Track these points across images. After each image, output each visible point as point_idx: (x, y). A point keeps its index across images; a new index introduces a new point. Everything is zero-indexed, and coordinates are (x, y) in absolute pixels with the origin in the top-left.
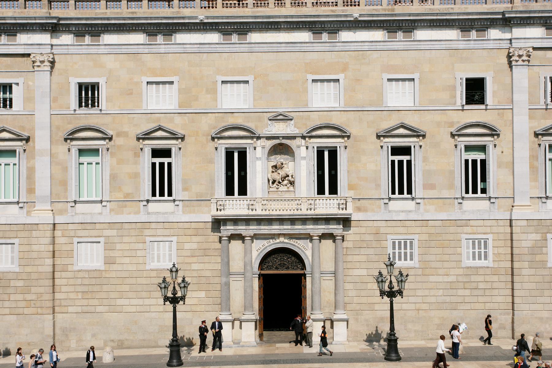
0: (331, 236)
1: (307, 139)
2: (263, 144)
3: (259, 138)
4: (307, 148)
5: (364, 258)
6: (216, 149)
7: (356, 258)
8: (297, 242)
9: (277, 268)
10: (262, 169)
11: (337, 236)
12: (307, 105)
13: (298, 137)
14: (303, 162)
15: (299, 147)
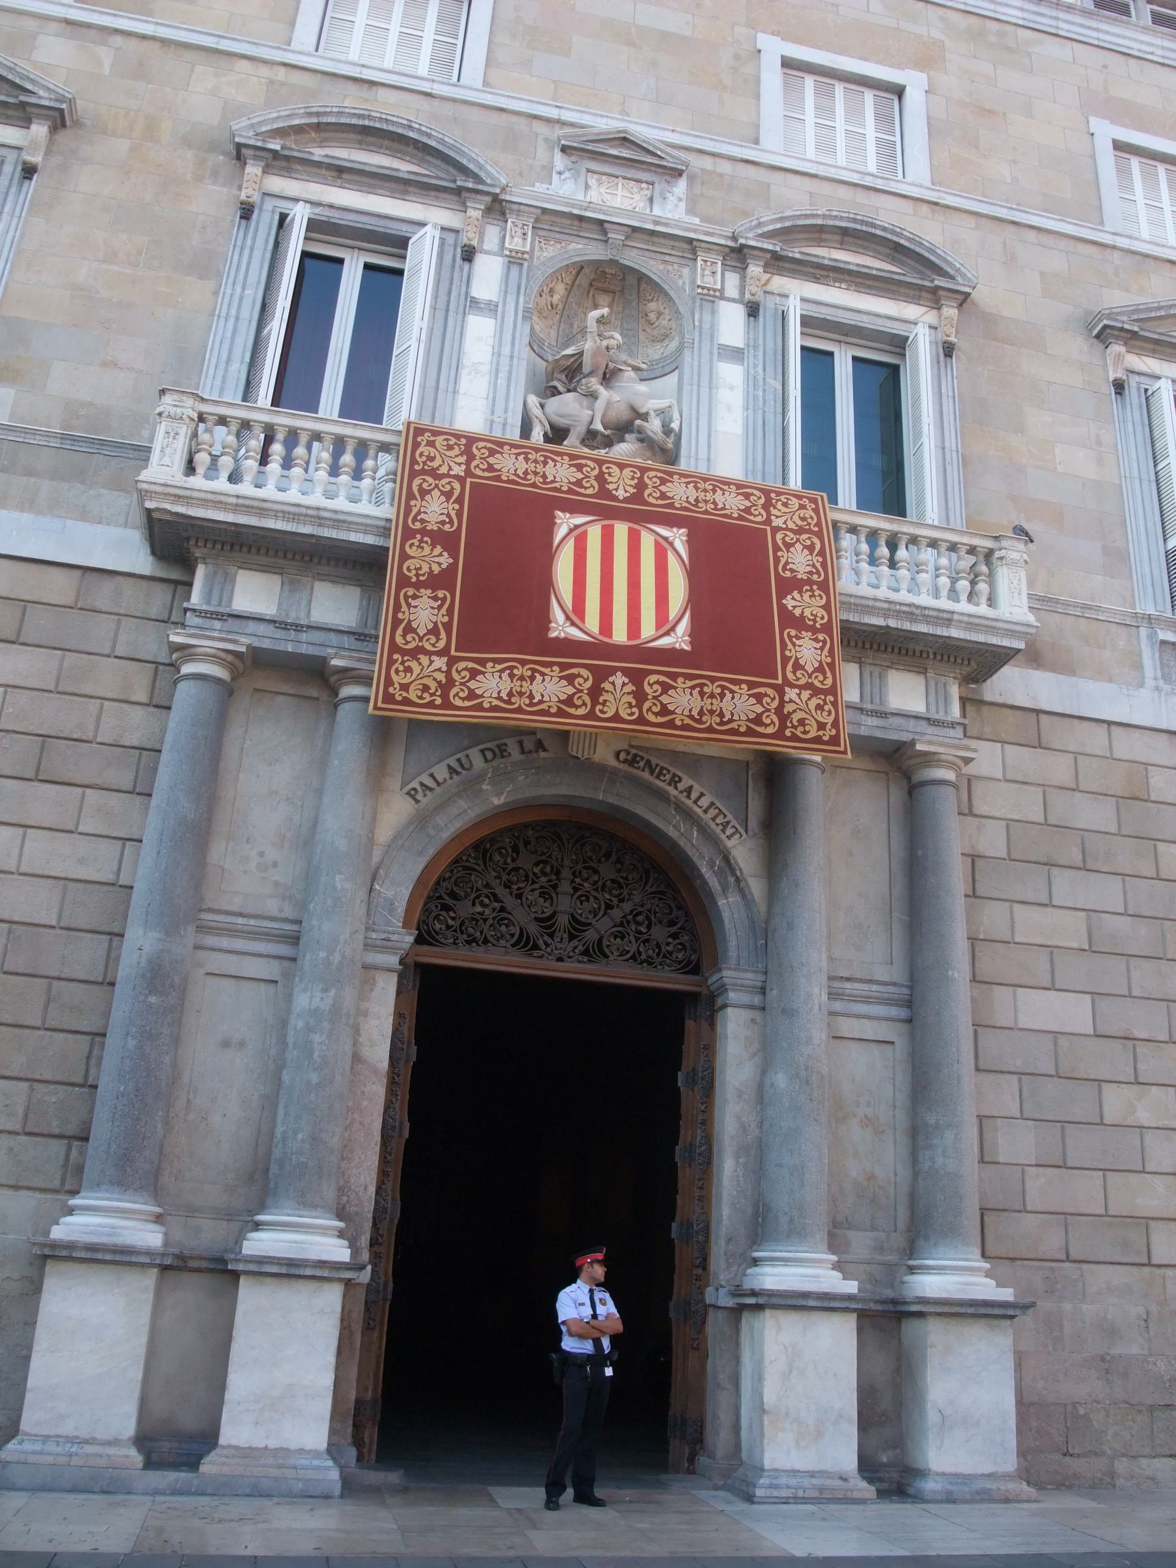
0: (895, 763)
1: (755, 269)
2: (515, 243)
3: (497, 208)
4: (753, 310)
5: (1069, 930)
6: (247, 212)
7: (1032, 924)
8: (675, 781)
9: (525, 943)
10: (497, 354)
11: (929, 759)
12: (756, 141)
13: (711, 247)
14: (731, 374)
15: (711, 297)
